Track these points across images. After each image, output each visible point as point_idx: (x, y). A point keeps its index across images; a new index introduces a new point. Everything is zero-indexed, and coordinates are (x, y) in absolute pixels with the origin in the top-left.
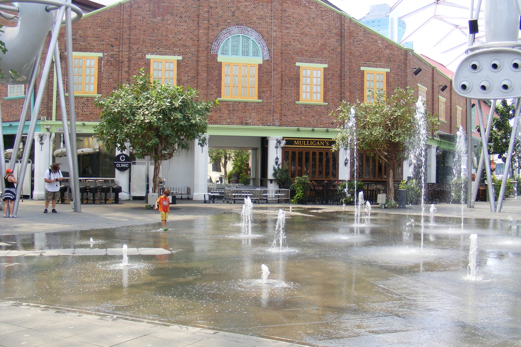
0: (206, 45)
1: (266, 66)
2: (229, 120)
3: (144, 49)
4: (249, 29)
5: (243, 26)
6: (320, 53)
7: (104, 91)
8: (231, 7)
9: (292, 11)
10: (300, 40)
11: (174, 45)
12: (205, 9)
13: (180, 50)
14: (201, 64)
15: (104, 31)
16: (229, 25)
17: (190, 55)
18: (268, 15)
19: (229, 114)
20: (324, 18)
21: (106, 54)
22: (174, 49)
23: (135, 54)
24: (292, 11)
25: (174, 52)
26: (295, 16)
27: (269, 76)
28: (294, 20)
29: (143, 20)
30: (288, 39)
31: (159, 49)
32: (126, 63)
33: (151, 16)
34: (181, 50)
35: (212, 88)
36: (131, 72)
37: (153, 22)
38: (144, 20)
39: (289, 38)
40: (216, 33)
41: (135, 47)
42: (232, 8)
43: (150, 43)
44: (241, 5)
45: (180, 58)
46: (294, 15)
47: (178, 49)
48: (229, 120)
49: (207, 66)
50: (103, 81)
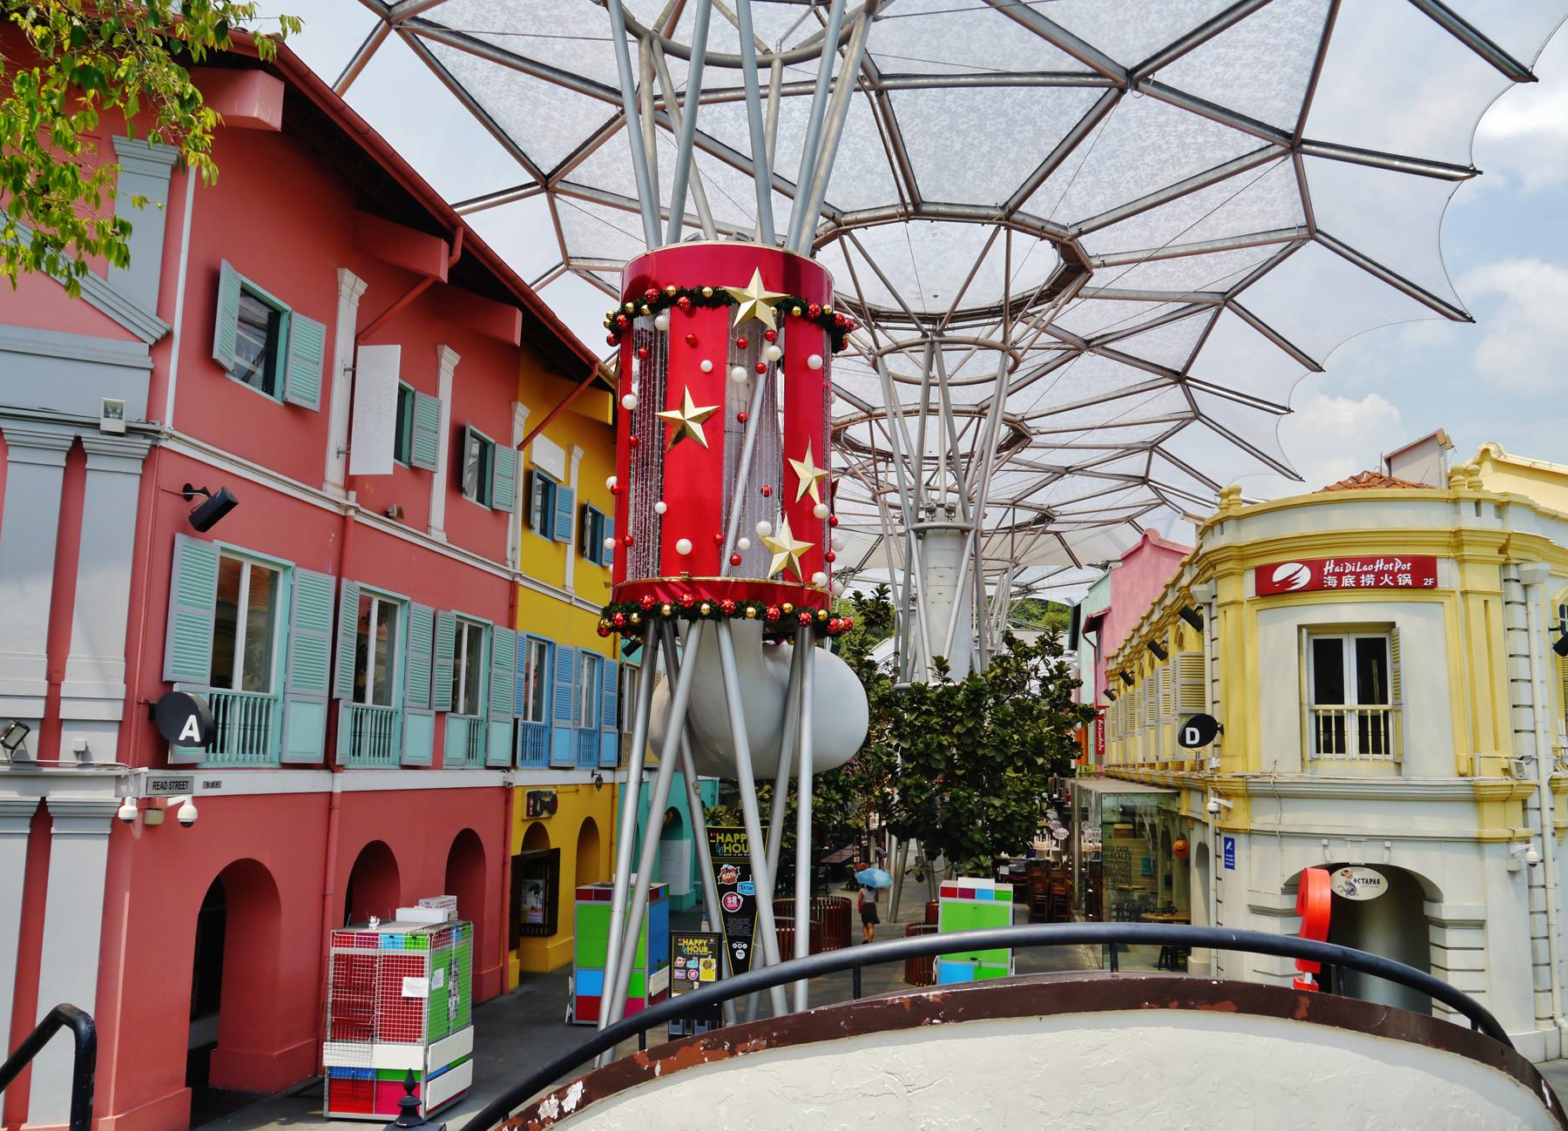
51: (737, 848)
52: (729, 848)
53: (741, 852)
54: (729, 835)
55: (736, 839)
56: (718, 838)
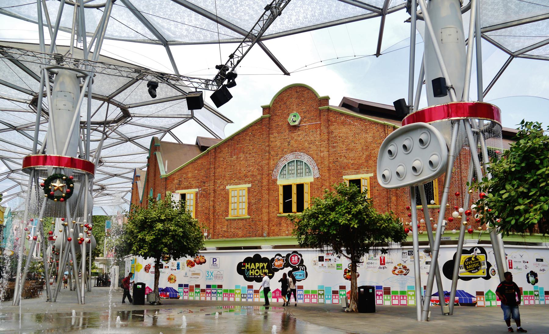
0: (267, 173)
1: (317, 183)
2: (287, 232)
3: (225, 182)
4: (302, 153)
5: (297, 152)
6: (365, 164)
7: (199, 216)
8: (287, 138)
9: (338, 131)
10: (347, 156)
11: (246, 176)
12: (266, 144)
13: (249, 179)
14: (264, 188)
15: (199, 173)
16: (286, 153)
17: (257, 182)
18: (317, 139)
19: (287, 227)
20: (368, 131)
21: (200, 189)
22: (246, 179)
23: (219, 187)
24: (338, 131)
25: (245, 181)
26: (341, 135)
27: (320, 191)
28: (340, 138)
29: (224, 161)
30: (335, 157)
31: (235, 181)
32: (212, 195)
33: (229, 156)
34: (250, 179)
35: (274, 207)
36: (216, 200)
37: (231, 161)
38: (225, 160)
39: (336, 155)
40: (276, 161)
41: (219, 182)
42: (288, 139)
43: (229, 177)
44: (295, 135)
45: (250, 185)
46: (340, 135)
47: (248, 179)
48: (287, 232)
49: (269, 189)
50: (199, 209)
51: (257, 272)
52: (253, 272)
53: (260, 275)
54: (253, 264)
55: (257, 266)
56: (247, 266)
